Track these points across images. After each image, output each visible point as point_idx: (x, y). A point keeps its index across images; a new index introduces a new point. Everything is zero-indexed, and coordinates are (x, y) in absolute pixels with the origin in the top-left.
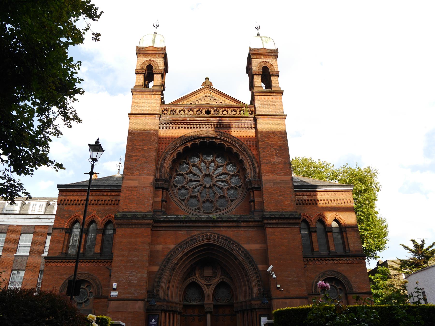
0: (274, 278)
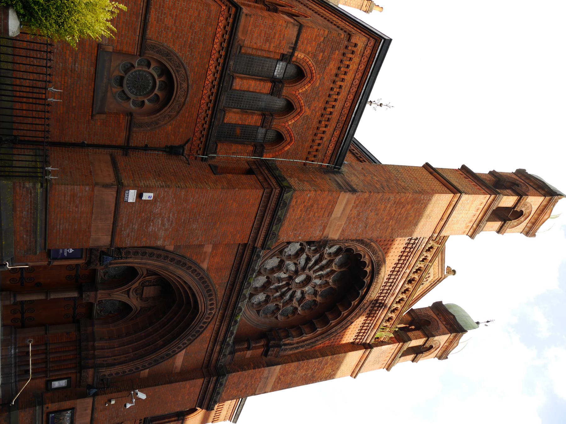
0: (125, 406)
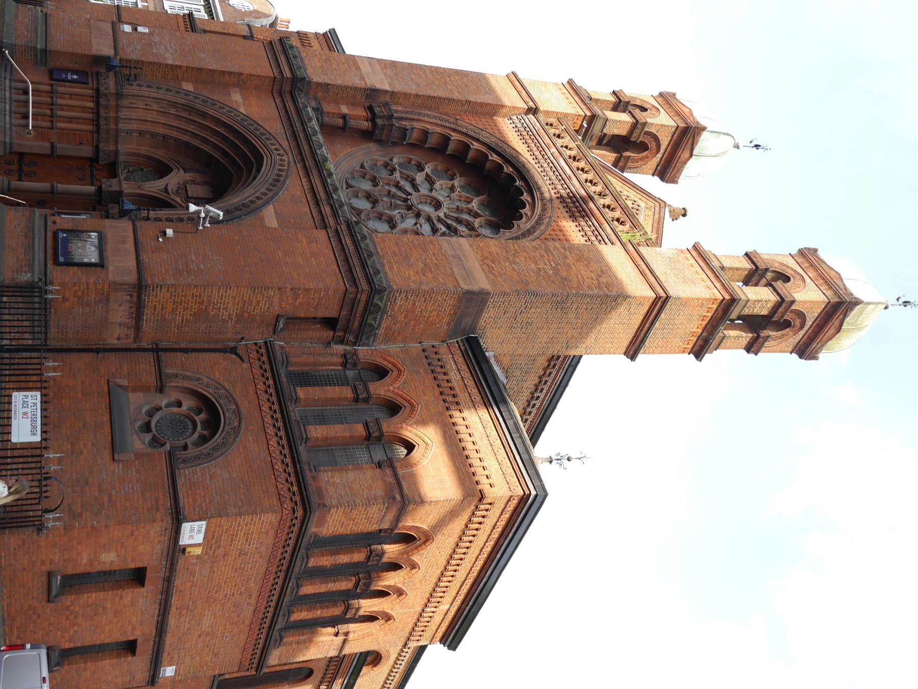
0: (187, 208)
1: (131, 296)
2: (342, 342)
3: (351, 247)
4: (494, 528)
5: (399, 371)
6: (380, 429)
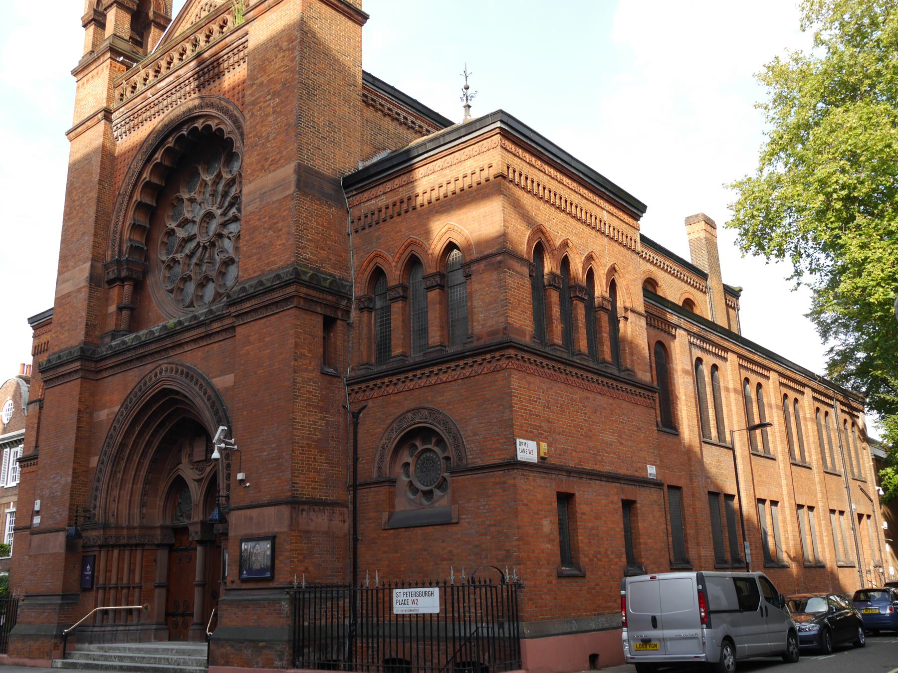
1: (303, 510)
2: (347, 312)
3: (254, 302)
4: (532, 165)
5: (376, 256)
6: (433, 275)
